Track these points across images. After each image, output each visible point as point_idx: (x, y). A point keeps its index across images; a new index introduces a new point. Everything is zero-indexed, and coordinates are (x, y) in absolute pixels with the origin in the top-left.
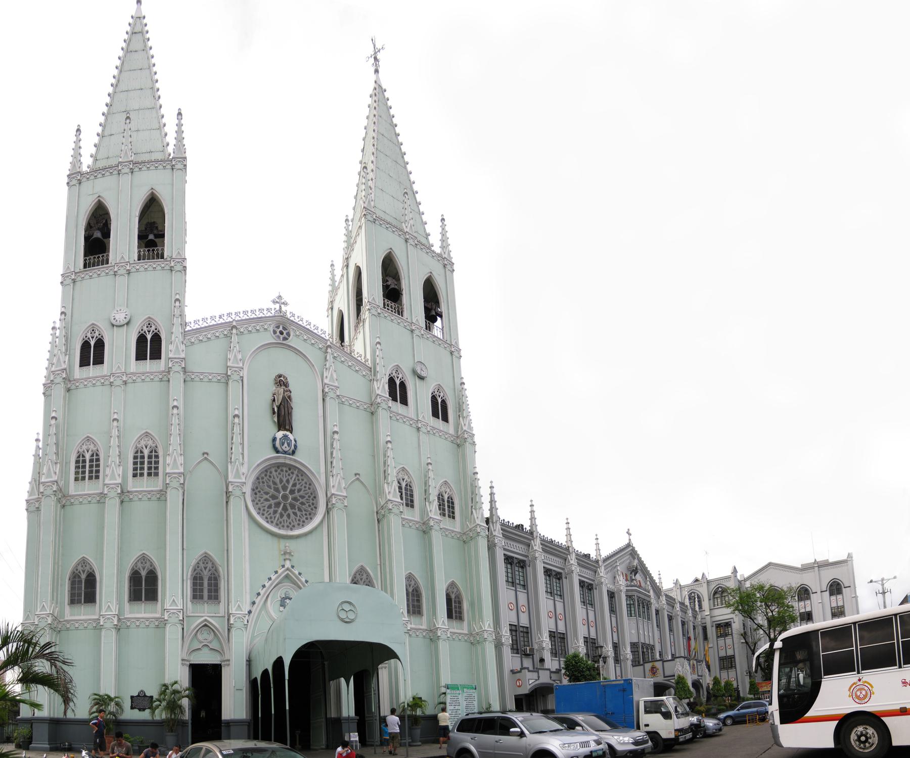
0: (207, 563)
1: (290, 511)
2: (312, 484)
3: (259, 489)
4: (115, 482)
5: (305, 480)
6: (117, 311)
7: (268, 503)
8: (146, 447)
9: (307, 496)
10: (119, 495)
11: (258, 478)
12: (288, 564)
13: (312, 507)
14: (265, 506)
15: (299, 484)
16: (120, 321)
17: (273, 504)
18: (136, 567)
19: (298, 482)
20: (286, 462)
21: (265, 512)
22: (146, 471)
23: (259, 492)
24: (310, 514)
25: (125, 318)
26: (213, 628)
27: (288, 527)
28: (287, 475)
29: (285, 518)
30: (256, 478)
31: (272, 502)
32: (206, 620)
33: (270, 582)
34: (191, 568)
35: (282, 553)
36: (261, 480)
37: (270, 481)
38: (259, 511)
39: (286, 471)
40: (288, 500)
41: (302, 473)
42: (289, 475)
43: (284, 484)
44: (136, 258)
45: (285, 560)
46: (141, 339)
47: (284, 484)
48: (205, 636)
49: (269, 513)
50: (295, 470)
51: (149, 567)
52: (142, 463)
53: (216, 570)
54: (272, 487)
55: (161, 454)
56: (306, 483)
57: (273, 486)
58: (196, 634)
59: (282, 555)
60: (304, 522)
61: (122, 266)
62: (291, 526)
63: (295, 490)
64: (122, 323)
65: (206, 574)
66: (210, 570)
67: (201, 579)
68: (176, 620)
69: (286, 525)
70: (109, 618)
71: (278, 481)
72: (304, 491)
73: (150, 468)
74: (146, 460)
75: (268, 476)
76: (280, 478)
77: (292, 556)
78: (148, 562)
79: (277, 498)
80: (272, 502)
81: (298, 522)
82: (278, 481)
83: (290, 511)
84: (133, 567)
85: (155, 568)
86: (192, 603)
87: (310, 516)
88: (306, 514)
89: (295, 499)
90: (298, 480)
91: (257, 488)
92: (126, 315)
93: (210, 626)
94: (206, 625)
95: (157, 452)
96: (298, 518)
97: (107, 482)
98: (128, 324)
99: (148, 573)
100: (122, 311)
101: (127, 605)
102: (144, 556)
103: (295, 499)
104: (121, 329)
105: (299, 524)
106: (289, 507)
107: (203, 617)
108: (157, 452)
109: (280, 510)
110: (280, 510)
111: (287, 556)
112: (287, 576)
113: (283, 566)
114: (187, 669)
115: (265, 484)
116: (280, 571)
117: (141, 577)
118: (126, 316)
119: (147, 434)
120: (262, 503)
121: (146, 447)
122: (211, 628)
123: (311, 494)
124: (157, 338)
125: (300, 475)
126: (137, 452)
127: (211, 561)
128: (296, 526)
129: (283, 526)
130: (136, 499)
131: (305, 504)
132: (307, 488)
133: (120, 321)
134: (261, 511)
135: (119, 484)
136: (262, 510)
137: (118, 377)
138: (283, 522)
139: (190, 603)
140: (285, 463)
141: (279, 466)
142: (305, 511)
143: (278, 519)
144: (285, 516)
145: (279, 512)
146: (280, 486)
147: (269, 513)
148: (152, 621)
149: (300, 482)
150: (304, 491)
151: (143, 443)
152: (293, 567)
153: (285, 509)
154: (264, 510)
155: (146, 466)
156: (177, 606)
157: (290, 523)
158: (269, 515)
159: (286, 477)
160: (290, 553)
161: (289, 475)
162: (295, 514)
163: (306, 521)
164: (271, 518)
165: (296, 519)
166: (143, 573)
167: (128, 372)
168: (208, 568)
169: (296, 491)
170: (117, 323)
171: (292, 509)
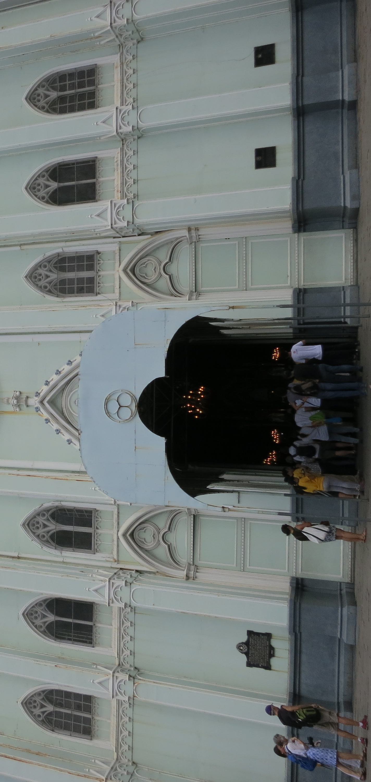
0: (38, 523)
18: (41, 627)
35: (18, 409)
53: (48, 510)
66: (48, 520)
68: (126, 590)
70: (119, 687)
78: (35, 609)
85: (45, 601)
99: (52, 612)
102: (27, 614)
112: (52, 402)
117: (57, 622)
122: (136, 528)
127: (35, 517)
152: (37, 394)
156: (104, 586)
166: (51, 618)
168: (46, 523)
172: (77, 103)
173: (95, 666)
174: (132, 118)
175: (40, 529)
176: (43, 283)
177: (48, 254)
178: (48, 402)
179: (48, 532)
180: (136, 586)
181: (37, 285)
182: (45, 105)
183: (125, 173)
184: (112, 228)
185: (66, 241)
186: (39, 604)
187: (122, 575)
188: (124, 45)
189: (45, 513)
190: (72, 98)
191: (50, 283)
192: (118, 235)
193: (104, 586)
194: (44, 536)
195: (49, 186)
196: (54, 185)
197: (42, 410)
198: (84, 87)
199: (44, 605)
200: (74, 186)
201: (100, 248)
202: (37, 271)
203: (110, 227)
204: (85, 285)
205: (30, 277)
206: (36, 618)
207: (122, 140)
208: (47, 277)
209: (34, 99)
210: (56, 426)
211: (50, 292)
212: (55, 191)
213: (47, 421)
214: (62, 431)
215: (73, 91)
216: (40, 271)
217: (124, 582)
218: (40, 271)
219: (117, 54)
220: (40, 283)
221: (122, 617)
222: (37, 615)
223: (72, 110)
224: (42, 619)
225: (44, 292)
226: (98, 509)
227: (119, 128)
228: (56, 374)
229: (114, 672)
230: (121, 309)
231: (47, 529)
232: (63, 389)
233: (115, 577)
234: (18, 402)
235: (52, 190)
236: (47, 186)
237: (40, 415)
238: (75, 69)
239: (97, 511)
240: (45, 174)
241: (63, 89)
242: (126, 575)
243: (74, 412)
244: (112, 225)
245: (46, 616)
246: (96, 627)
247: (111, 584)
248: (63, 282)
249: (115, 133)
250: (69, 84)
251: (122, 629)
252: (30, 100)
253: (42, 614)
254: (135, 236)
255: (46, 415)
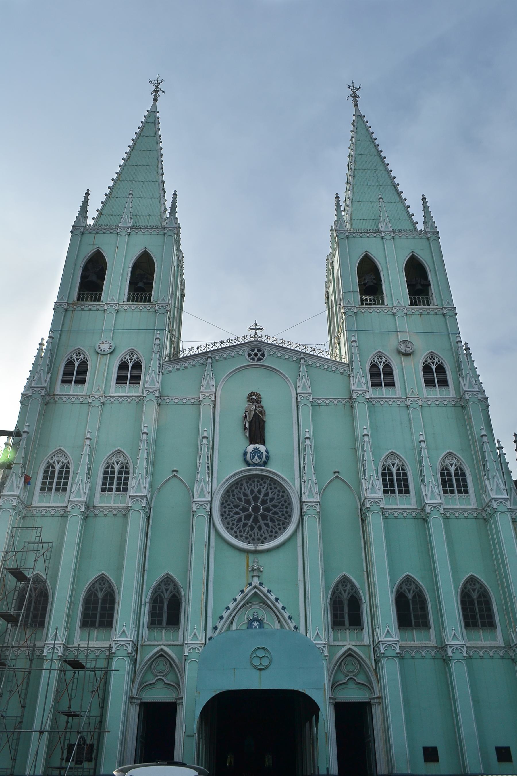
0: (169, 585)
1: (261, 522)
2: (286, 492)
3: (229, 502)
4: (80, 500)
5: (278, 488)
6: (103, 342)
7: (238, 516)
8: (117, 463)
9: (280, 505)
10: (82, 513)
11: (228, 492)
12: (256, 582)
13: (286, 515)
14: (234, 520)
15: (272, 493)
16: (104, 351)
17: (243, 517)
18: (94, 588)
19: (270, 491)
20: (258, 473)
21: (234, 527)
22: (114, 487)
23: (229, 505)
24: (283, 524)
25: (109, 348)
26: (170, 660)
27: (259, 539)
28: (259, 485)
29: (256, 530)
30: (225, 491)
31: (242, 514)
32: (162, 650)
33: (235, 603)
34: (151, 590)
35: (250, 569)
36: (231, 493)
37: (240, 493)
38: (228, 526)
39: (258, 482)
40: (259, 511)
41: (276, 482)
42: (261, 485)
43: (256, 495)
44: (126, 300)
45: (253, 577)
46: (123, 365)
47: (256, 495)
48: (161, 666)
49: (238, 527)
50: (268, 479)
51: (107, 588)
52: (112, 478)
53: (178, 592)
54: (243, 499)
55: (131, 470)
56: (279, 491)
57: (243, 498)
58: (150, 666)
59: (250, 571)
60: (276, 533)
61: (112, 306)
62: (262, 539)
63: (267, 500)
64: (106, 352)
65: (167, 596)
66: (171, 592)
67: (162, 602)
69: (256, 538)
71: (248, 492)
72: (277, 499)
73: (119, 484)
74: (116, 475)
75: (239, 489)
76: (252, 489)
77: (262, 571)
79: (248, 510)
80: (242, 514)
81: (270, 533)
82: (248, 492)
83: (261, 522)
84: (90, 588)
86: (149, 630)
87: (284, 526)
88: (279, 525)
89: (267, 510)
90: (271, 489)
91: (226, 501)
92: (110, 346)
93: (166, 656)
94: (161, 655)
95: (128, 469)
96: (271, 529)
97: (72, 499)
98: (111, 353)
100: (107, 343)
101: (78, 631)
102: (103, 577)
103: (267, 510)
104: (105, 356)
105: (271, 536)
106: (260, 519)
107: (159, 645)
108: (128, 469)
109: (250, 522)
110: (250, 522)
111: (255, 573)
113: (250, 584)
114: (138, 708)
115: (236, 497)
116: (246, 591)
117: (98, 600)
118: (110, 347)
119: (119, 452)
120: (232, 517)
121: (117, 463)
123: (285, 502)
124: (138, 365)
125: (272, 484)
126: (108, 468)
128: (268, 538)
129: (253, 539)
130: (101, 515)
131: (278, 514)
132: (280, 496)
133: (104, 351)
134: (230, 526)
135: (84, 502)
136: (231, 524)
137: (97, 398)
138: (253, 535)
139: (147, 629)
140: (256, 474)
141: (250, 478)
142: (278, 520)
143: (248, 532)
144: (256, 528)
145: (249, 524)
146: (251, 497)
147: (238, 527)
148: (103, 651)
149: (272, 490)
150: (277, 499)
151: (114, 459)
152: (261, 584)
153: (256, 521)
154: (233, 524)
155: (115, 482)
157: (261, 536)
158: (238, 529)
159: (258, 487)
160: (258, 569)
161: (261, 485)
162: (267, 525)
163: (279, 531)
164: (240, 532)
165: (267, 531)
166: (100, 595)
167: (107, 394)
168: (169, 591)
169: (268, 501)
170: (102, 352)
171: (263, 520)
172: (469, 613)
173: (67, 629)
174: (457, 656)
175: (165, 586)
176: (340, 588)
177: (361, 593)
178: (256, 592)
179: (162, 592)
180: (127, 661)
181: (339, 583)
182: (468, 589)
183: (419, 650)
184: (380, 641)
185: (370, 605)
186: (110, 586)
187: (134, 649)
188: (511, 649)
189: (177, 590)
190: (473, 610)
191: (340, 593)
192: (375, 645)
193: (127, 637)
194: (159, 589)
195: (409, 592)
196: (410, 596)
197: (250, 587)
198: (480, 619)
199: (109, 590)
200: (410, 611)
201: (365, 631)
202: (349, 584)
203: (380, 640)
204: (339, 619)
205: (344, 578)
206: (100, 584)
207: (442, 648)
208: (345, 591)
209: (472, 581)
210: (239, 598)
211: (334, 593)
212: (406, 597)
213: (242, 592)
214: (235, 603)
215: (477, 610)
216: (349, 586)
217: (130, 652)
218: (349, 586)
219: (504, 644)
220: (340, 586)
221: (102, 649)
222: (102, 584)
223: (464, 609)
224: (99, 588)
225: (334, 588)
226: (180, 630)
227: (450, 646)
228: (276, 598)
229: (63, 644)
230: (322, 647)
231: (165, 592)
232: (265, 603)
233: (133, 645)
234: (255, 569)
235: (406, 594)
236: (409, 591)
237: (246, 586)
238: (494, 612)
239: (178, 629)
240: (418, 590)
241: (479, 603)
242: (134, 651)
243: (249, 611)
244: (382, 641)
245: (101, 592)
246: (95, 629)
247: (128, 642)
248: (341, 602)
249: (447, 643)
250: (483, 608)
251: (94, 649)
252: (471, 578)
253: (104, 588)
254: (374, 657)
255: (246, 591)
